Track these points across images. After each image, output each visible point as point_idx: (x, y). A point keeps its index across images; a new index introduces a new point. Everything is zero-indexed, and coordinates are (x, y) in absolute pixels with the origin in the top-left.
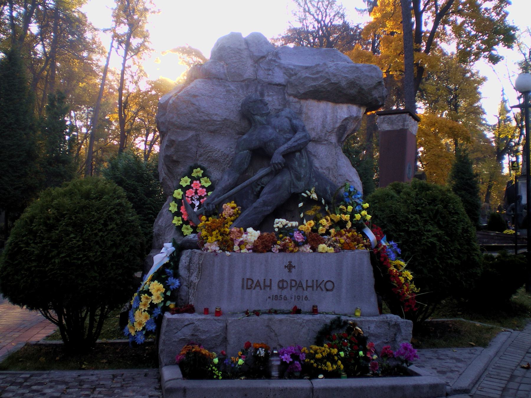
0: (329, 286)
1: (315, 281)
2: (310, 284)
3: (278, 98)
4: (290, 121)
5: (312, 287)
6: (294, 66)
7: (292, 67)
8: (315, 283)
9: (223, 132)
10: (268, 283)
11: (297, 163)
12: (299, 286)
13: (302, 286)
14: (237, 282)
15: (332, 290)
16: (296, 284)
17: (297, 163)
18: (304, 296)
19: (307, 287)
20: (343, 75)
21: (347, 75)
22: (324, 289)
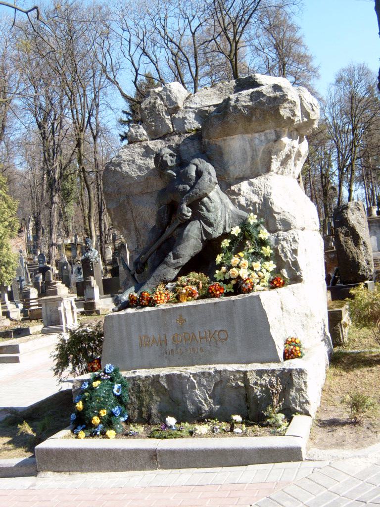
0: (223, 336)
1: (207, 332)
2: (203, 335)
3: (193, 145)
4: (197, 166)
5: (206, 338)
6: (209, 106)
7: (207, 108)
8: (208, 334)
9: (149, 191)
10: (163, 338)
11: (204, 209)
12: (192, 338)
13: (196, 339)
14: (136, 340)
15: (226, 339)
16: (190, 337)
17: (204, 209)
18: (199, 348)
19: (201, 338)
20: (244, 104)
21: (249, 104)
22: (218, 339)
